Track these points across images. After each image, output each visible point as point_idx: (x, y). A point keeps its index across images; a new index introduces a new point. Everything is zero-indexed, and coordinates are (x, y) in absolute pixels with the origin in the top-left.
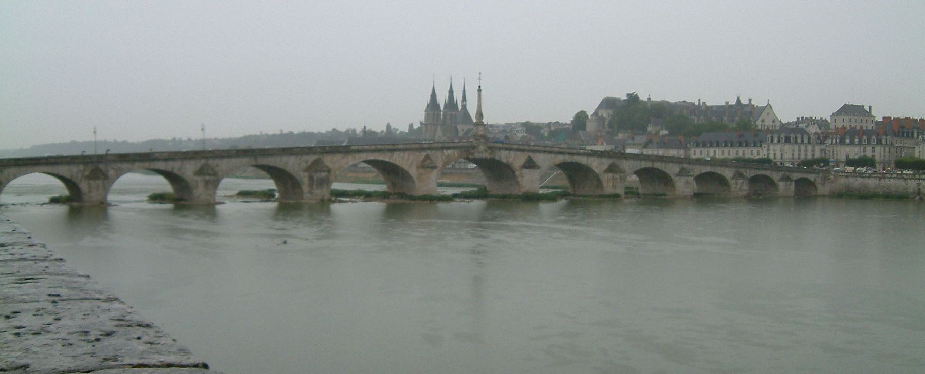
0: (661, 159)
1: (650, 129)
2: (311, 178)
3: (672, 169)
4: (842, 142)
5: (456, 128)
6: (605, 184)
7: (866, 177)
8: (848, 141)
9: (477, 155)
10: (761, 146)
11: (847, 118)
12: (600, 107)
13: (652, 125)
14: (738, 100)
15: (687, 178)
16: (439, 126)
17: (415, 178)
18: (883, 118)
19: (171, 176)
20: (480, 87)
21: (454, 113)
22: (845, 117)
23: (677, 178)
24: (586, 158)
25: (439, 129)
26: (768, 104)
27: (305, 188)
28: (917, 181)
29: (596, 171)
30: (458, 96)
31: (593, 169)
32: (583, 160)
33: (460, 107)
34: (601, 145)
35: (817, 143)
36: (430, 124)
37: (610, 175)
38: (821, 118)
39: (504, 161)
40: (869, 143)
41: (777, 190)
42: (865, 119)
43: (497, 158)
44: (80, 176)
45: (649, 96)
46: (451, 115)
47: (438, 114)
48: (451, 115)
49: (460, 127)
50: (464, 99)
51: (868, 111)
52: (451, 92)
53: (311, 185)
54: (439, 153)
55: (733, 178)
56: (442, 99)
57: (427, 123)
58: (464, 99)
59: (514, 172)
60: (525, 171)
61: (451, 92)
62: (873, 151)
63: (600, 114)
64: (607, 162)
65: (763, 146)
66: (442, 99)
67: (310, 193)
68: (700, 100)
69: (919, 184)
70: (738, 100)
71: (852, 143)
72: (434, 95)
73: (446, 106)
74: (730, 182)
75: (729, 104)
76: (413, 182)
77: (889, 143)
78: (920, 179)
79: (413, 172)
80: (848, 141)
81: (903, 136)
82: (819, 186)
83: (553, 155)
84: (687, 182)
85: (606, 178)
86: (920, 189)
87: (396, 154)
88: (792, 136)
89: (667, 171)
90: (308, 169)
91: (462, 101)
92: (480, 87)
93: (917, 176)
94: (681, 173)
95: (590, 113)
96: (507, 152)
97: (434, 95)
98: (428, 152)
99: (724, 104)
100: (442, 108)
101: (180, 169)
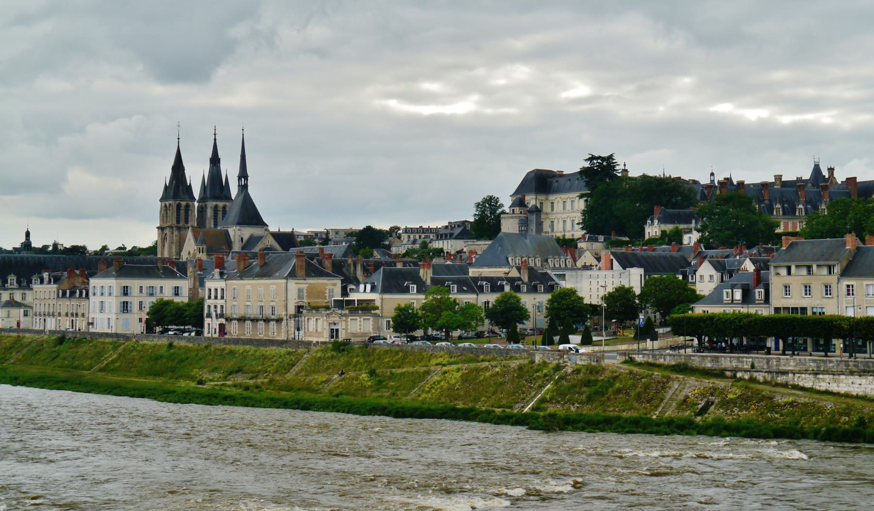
1: (652, 230)
5: (227, 234)
13: (656, 222)
16: (190, 228)
21: (221, 204)
25: (190, 235)
30: (230, 170)
33: (234, 191)
34: (606, 269)
36: (171, 227)
45: (625, 165)
46: (216, 207)
47: (187, 206)
48: (216, 207)
49: (234, 232)
50: (243, 174)
52: (215, 160)
57: (165, 225)
58: (243, 174)
61: (215, 160)
68: (712, 174)
72: (178, 167)
73: (204, 188)
75: (783, 179)
91: (240, 178)
95: (506, 202)
97: (178, 167)
99: (773, 181)
100: (197, 192)
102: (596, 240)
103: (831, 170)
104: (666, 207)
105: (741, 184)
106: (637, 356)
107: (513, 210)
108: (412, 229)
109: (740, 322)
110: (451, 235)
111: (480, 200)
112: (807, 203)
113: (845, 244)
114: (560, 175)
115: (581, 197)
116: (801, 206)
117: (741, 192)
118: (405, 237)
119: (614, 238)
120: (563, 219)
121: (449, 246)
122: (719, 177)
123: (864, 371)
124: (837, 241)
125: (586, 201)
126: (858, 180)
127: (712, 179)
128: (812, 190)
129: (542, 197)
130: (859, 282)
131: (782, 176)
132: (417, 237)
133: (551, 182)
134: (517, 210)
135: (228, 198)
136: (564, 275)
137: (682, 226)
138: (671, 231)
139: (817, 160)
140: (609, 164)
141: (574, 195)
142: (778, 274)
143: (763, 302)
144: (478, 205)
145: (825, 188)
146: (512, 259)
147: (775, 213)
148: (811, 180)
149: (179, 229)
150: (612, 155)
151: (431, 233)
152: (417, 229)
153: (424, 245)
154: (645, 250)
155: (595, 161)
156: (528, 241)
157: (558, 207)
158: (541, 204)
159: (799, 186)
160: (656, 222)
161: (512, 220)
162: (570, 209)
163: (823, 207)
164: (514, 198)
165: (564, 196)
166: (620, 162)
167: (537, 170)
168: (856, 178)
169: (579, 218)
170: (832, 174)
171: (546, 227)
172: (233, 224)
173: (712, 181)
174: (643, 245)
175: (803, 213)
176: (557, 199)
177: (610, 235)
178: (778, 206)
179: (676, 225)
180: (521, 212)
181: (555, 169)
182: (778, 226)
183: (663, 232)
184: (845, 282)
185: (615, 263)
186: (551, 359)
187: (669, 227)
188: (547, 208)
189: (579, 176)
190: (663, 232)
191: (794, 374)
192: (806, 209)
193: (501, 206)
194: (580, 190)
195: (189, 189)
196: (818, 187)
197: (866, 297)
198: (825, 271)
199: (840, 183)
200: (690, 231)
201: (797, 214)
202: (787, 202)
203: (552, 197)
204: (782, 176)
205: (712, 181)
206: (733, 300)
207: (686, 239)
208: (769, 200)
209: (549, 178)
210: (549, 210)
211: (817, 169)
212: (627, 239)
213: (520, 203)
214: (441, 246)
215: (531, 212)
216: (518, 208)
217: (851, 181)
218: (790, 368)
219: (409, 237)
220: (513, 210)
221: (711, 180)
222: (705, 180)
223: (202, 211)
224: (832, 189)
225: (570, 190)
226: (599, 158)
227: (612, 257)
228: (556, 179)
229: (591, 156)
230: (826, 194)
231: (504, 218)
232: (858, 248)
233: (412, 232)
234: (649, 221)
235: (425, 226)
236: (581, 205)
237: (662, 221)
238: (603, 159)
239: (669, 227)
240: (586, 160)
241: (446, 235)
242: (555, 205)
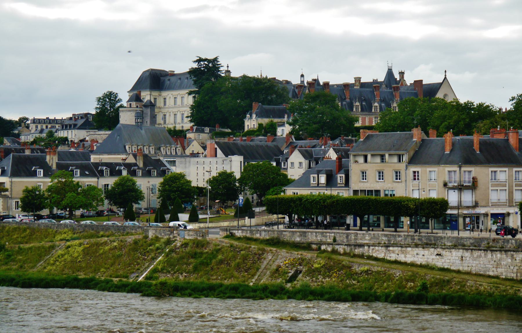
12: (139, 85)
13: (254, 116)
26: (445, 78)
34: (211, 156)
45: (228, 67)
68: (302, 76)
75: (362, 81)
95: (124, 97)
99: (353, 82)
102: (203, 131)
103: (402, 74)
104: (263, 104)
105: (326, 84)
106: (237, 231)
107: (130, 104)
108: (39, 119)
109: (324, 202)
110: (75, 125)
111: (101, 95)
112: (381, 101)
113: (412, 137)
114: (172, 74)
115: (190, 93)
116: (376, 104)
117: (327, 91)
118: (33, 127)
119: (218, 129)
120: (174, 113)
121: (74, 135)
122: (308, 79)
123: (427, 244)
124: (406, 134)
125: (194, 97)
126: (424, 83)
127: (302, 79)
128: (386, 90)
129: (155, 93)
130: (424, 169)
131: (360, 78)
132: (44, 127)
133: (164, 81)
134: (134, 104)
136: (175, 161)
137: (276, 120)
138: (267, 124)
139: (390, 65)
140: (214, 66)
141: (185, 92)
142: (356, 162)
143: (343, 185)
144: (99, 99)
145: (397, 89)
146: (129, 147)
147: (354, 110)
148: (385, 82)
150: (216, 58)
151: (57, 123)
152: (44, 120)
153: (51, 134)
154: (245, 140)
155: (202, 63)
156: (143, 132)
157: (170, 102)
158: (155, 99)
159: (375, 87)
160: (254, 116)
161: (129, 113)
162: (180, 104)
163: (395, 105)
164: (131, 94)
165: (175, 93)
166: (224, 64)
167: (152, 70)
168: (422, 81)
169: (188, 112)
170: (403, 77)
171: (159, 119)
173: (302, 82)
174: (243, 136)
175: (378, 110)
176: (169, 95)
177: (215, 127)
178: (358, 104)
179: (271, 119)
180: (137, 107)
181: (167, 70)
182: (357, 121)
183: (260, 125)
184: (412, 169)
185: (219, 151)
186: (163, 234)
187: (265, 121)
188: (160, 103)
189: (188, 76)
190: (260, 125)
191: (369, 246)
192: (380, 106)
193: (120, 100)
194: (189, 87)
196: (391, 88)
197: (429, 182)
198: (395, 159)
199: (409, 85)
200: (283, 125)
201: (373, 111)
202: (365, 100)
203: (165, 94)
204: (360, 78)
205: (302, 82)
206: (318, 184)
207: (279, 131)
208: (350, 98)
209: (162, 76)
210: (162, 105)
211: (390, 73)
212: (229, 131)
213: (137, 98)
214: (65, 135)
215: (146, 106)
216: (134, 103)
217: (418, 83)
218: (365, 242)
219: (37, 127)
220: (130, 104)
221: (301, 81)
222: (296, 81)
224: (402, 90)
225: (180, 88)
226: (206, 60)
227: (216, 146)
228: (168, 78)
229: (198, 58)
230: (398, 94)
231: (123, 111)
232: (423, 140)
233: (39, 123)
234: (248, 116)
235: (52, 117)
236: (190, 100)
237: (260, 115)
238: (209, 61)
239: (265, 121)
240: (194, 62)
241: (70, 126)
242: (167, 101)
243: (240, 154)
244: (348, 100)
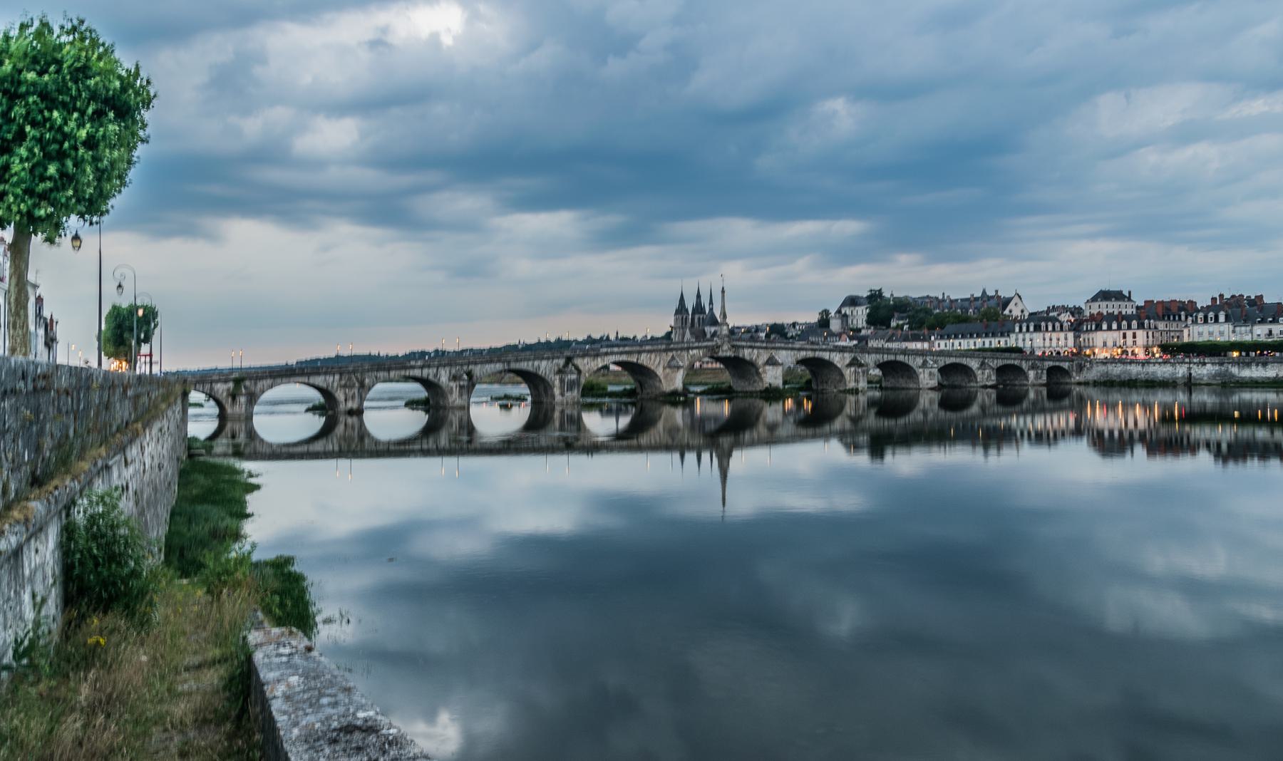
0: (905, 352)
1: (893, 324)
2: (562, 381)
3: (915, 362)
4: (1099, 328)
6: (847, 377)
7: (1127, 363)
8: (1105, 326)
9: (720, 354)
10: (1008, 336)
11: (1104, 304)
12: (844, 304)
14: (984, 292)
15: (930, 370)
17: (662, 377)
18: (1145, 302)
19: (425, 382)
20: (723, 288)
22: (1101, 303)
23: (921, 370)
24: (828, 353)
27: (557, 391)
28: (1187, 366)
29: (839, 365)
30: (705, 301)
31: (835, 363)
32: (826, 355)
35: (1070, 330)
37: (853, 369)
38: (1074, 306)
39: (747, 357)
40: (1129, 327)
41: (1027, 378)
42: (1123, 304)
43: (741, 355)
44: (335, 384)
50: (711, 303)
51: (1128, 295)
52: (699, 296)
53: (562, 388)
54: (685, 353)
55: (979, 369)
56: (690, 304)
58: (711, 303)
59: (757, 370)
60: (767, 367)
61: (699, 296)
62: (1134, 336)
63: (843, 312)
64: (848, 357)
65: (1011, 335)
66: (690, 304)
67: (562, 394)
68: (943, 294)
69: (1189, 369)
70: (984, 292)
71: (1110, 328)
73: (693, 309)
74: (976, 372)
75: (975, 296)
76: (660, 381)
77: (1152, 326)
78: (1190, 363)
79: (660, 372)
80: (1105, 326)
81: (1169, 318)
82: (1074, 374)
83: (796, 352)
84: (930, 374)
85: (848, 373)
86: (1190, 374)
87: (643, 356)
88: (1043, 324)
89: (911, 363)
90: (560, 372)
92: (723, 288)
93: (1187, 360)
94: (924, 364)
95: (833, 312)
96: (750, 350)
98: (674, 352)
100: (690, 313)
101: (435, 376)
104: (901, 312)
111: (820, 311)
129: (852, 308)
134: (837, 315)
135: (705, 313)
141: (864, 307)
149: (683, 328)
157: (860, 313)
169: (865, 318)
171: (850, 322)
172: (707, 325)
187: (901, 322)
188: (855, 313)
192: (974, 312)
195: (687, 310)
203: (857, 308)
213: (839, 312)
223: (693, 319)
237: (899, 319)
239: (901, 322)
243: (856, 340)
244: (954, 309)
